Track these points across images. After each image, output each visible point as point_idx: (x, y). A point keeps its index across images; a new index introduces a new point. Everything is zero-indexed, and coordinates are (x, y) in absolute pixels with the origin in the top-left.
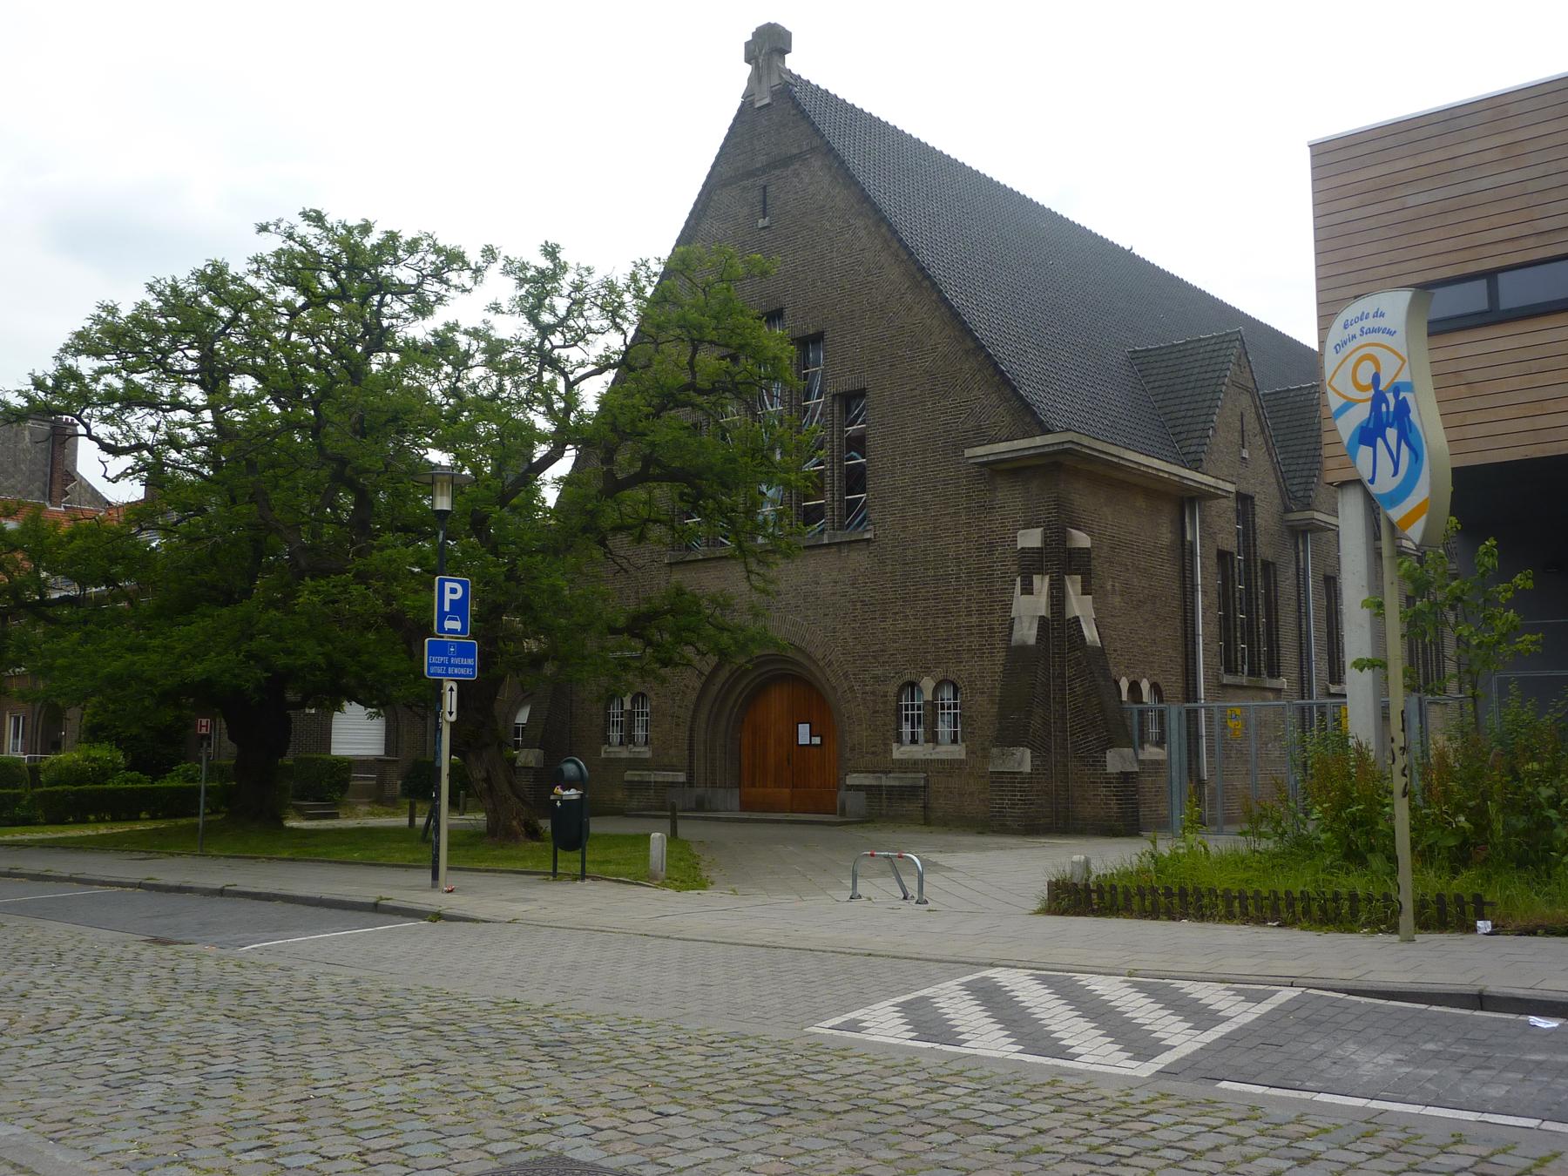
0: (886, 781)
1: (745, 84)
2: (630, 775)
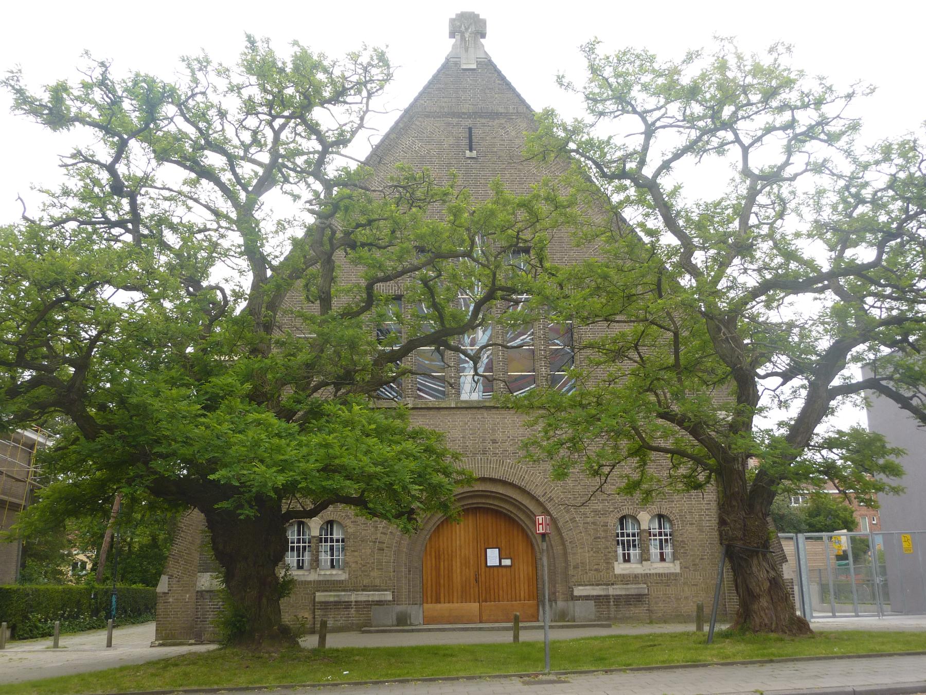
0: (612, 591)
1: (450, 49)
2: (320, 596)
